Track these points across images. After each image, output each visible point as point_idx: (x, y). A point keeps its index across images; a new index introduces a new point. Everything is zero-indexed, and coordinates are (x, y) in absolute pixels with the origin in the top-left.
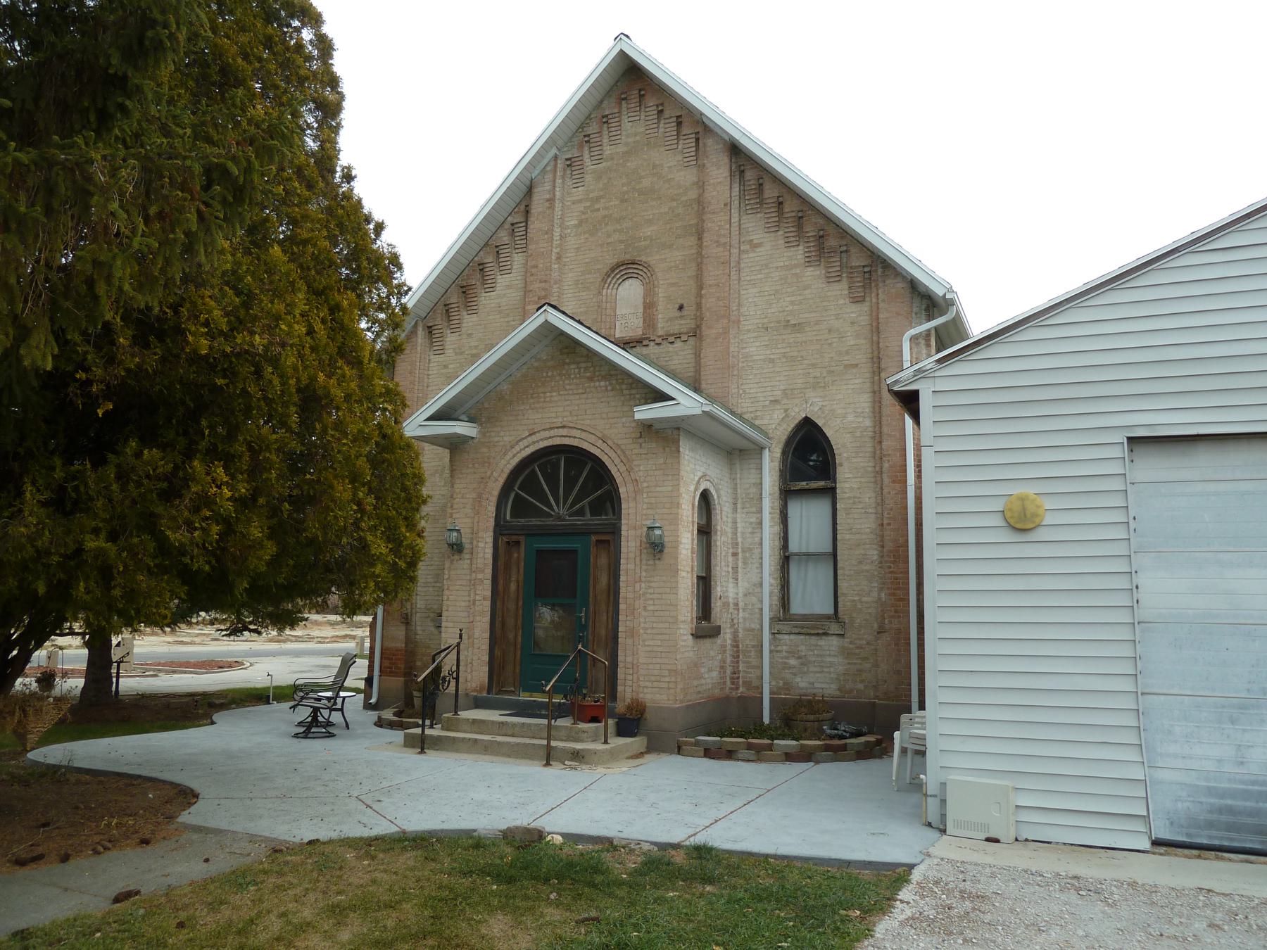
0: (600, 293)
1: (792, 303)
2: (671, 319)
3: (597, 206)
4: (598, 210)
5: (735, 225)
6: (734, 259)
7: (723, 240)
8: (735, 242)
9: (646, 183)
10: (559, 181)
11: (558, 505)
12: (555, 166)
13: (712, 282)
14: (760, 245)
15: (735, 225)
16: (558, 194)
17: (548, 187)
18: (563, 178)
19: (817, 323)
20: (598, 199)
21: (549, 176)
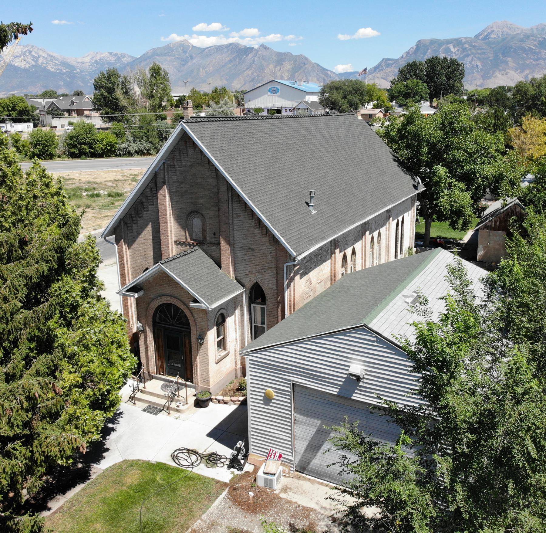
0: (186, 222)
1: (251, 241)
2: (211, 237)
3: (182, 186)
4: (182, 187)
5: (230, 208)
6: (230, 222)
7: (226, 214)
8: (231, 215)
9: (199, 180)
10: (166, 173)
11: (169, 319)
12: (164, 168)
13: (223, 230)
14: (240, 216)
15: (230, 208)
16: (166, 179)
17: (162, 176)
18: (168, 171)
19: (259, 250)
20: (182, 183)
21: (162, 172)
